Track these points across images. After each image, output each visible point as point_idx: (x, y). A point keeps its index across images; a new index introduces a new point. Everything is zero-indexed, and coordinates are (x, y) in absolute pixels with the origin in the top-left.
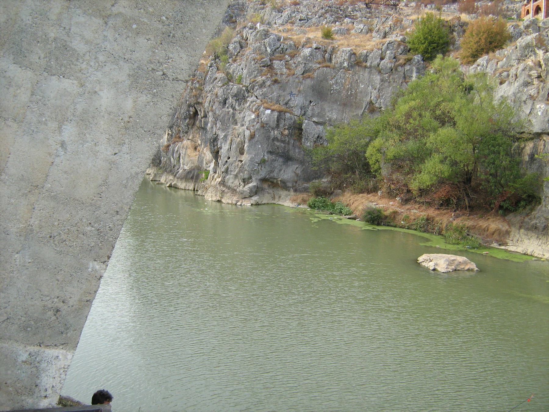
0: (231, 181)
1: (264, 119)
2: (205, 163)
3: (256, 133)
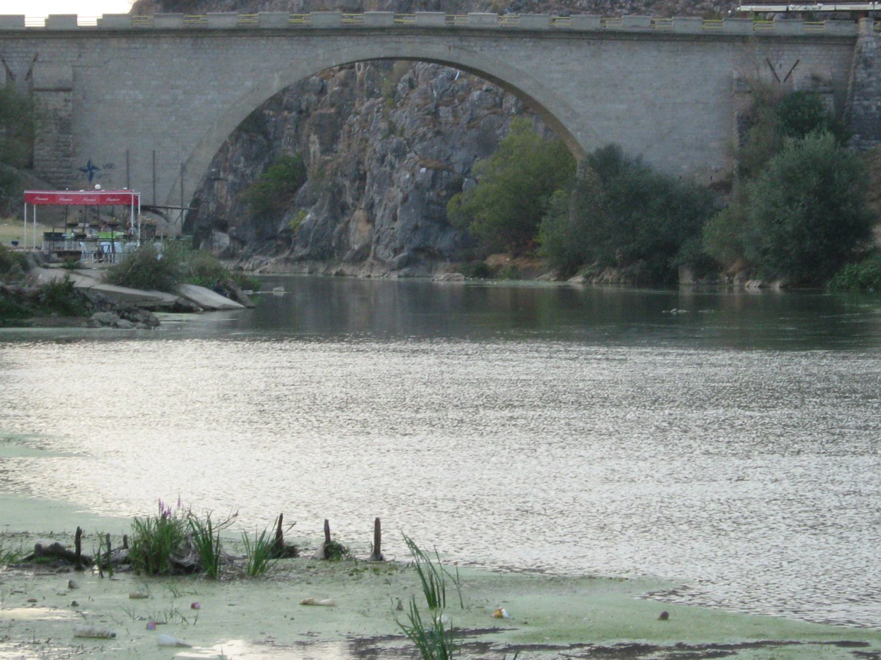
0: (381, 252)
1: (418, 178)
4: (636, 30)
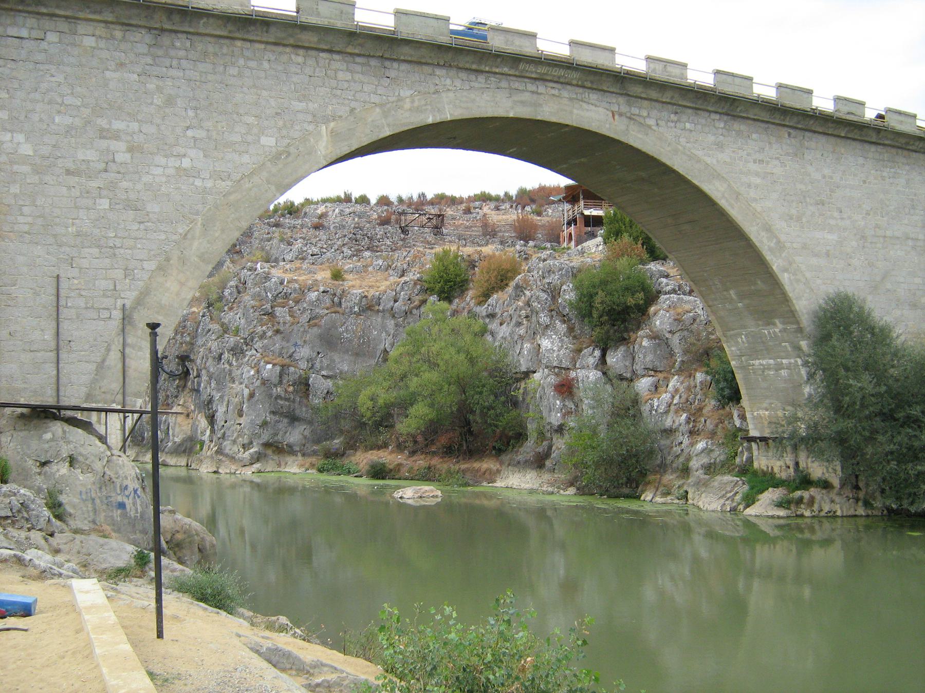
0: (228, 448)
1: (265, 375)
2: (199, 432)
3: (256, 391)
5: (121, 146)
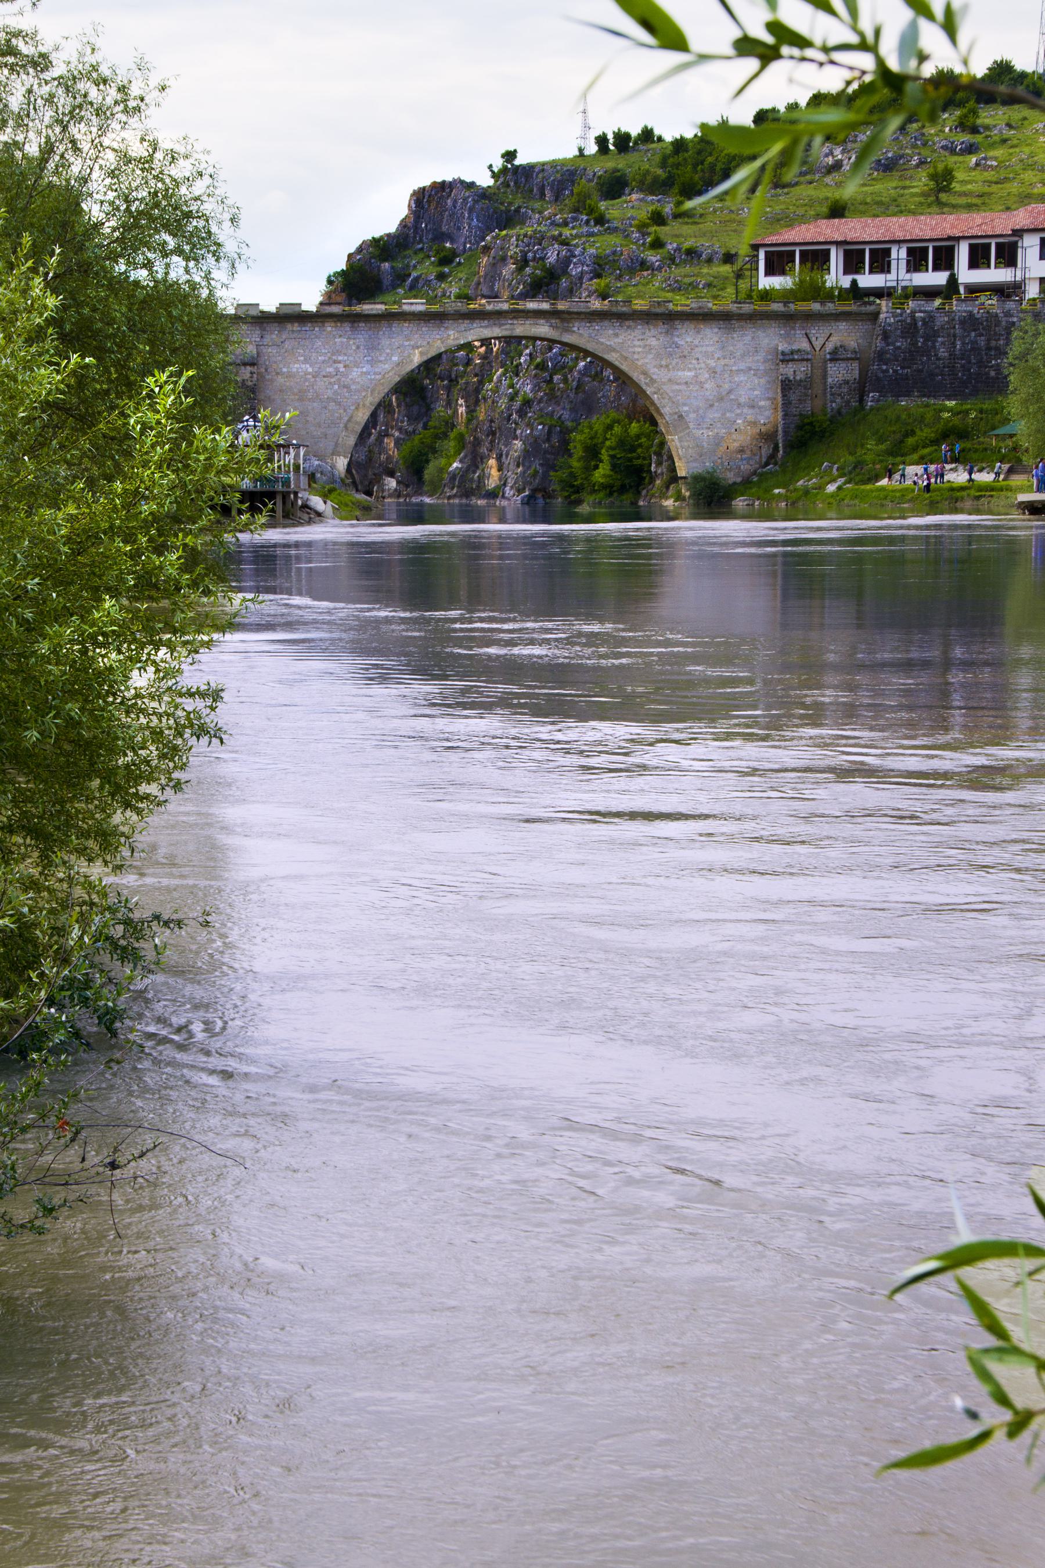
1: (536, 433)
4: (701, 311)
5: (341, 366)
